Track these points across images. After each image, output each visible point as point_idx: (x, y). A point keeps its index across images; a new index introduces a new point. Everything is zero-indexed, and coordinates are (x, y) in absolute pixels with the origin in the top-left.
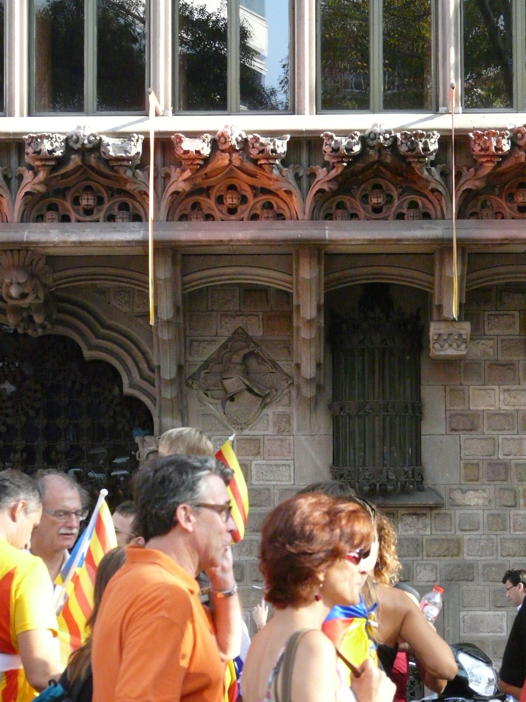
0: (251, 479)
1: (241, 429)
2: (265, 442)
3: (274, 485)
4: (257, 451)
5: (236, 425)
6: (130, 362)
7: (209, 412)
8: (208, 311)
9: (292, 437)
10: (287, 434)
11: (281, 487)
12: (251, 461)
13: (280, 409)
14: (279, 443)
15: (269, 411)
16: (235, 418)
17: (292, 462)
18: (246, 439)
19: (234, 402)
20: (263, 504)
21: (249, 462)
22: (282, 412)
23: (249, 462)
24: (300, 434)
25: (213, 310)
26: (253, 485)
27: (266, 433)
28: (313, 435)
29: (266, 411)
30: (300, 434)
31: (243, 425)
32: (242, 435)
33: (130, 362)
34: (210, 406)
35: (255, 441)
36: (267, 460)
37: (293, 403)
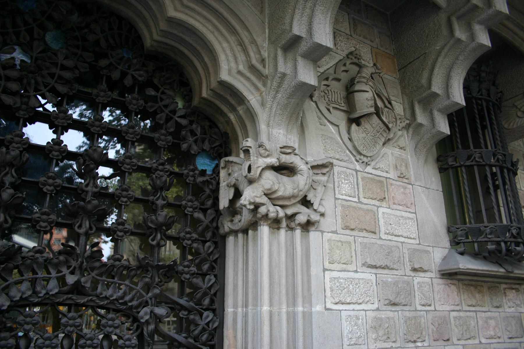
0: (380, 231)
2: (388, 186)
3: (402, 242)
5: (362, 157)
9: (410, 186)
10: (406, 181)
11: (409, 246)
12: (378, 207)
13: (397, 152)
14: (402, 190)
17: (415, 215)
19: (360, 127)
20: (395, 266)
26: (382, 239)
28: (428, 188)
31: (369, 158)
32: (365, 172)
34: (331, 126)
35: (381, 183)
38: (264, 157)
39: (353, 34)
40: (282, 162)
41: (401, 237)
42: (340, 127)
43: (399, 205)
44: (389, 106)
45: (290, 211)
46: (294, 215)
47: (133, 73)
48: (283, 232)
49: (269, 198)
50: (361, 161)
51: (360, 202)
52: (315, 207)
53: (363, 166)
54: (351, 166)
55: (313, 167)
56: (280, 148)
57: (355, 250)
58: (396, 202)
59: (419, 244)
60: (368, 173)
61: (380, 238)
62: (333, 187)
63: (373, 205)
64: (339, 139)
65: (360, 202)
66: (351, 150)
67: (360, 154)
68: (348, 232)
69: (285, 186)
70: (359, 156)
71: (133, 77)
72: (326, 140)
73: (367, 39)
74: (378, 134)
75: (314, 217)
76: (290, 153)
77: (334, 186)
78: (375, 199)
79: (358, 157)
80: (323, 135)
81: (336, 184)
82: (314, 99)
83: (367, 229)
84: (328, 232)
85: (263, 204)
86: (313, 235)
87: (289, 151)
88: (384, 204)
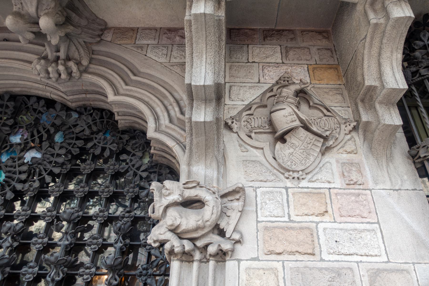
0: (321, 251)
1: (298, 178)
3: (357, 262)
4: (323, 209)
5: (291, 173)
6: (160, 110)
7: (254, 159)
8: (248, 62)
9: (368, 192)
11: (370, 266)
12: (317, 223)
15: (331, 158)
16: (289, 163)
18: (306, 193)
21: (314, 225)
22: (348, 160)
23: (314, 225)
24: (378, 187)
25: (254, 62)
26: (324, 260)
27: (332, 186)
28: (397, 190)
29: (328, 158)
30: (378, 187)
31: (300, 172)
32: (299, 187)
33: (160, 110)
34: (254, 150)
36: (340, 223)
37: (360, 151)
38: (167, 196)
39: (285, 61)
40: (186, 197)
41: (355, 256)
42: (264, 149)
43: (350, 216)
44: (328, 114)
45: (200, 244)
46: (206, 246)
47: (110, 146)
48: (195, 265)
49: (175, 233)
50: (291, 178)
51: (291, 221)
52: (228, 235)
53: (296, 182)
54: (282, 185)
55: (223, 196)
56: (184, 184)
57: (284, 278)
58: (344, 213)
59: (389, 262)
60: (302, 188)
61: (322, 260)
62: (255, 210)
63: (310, 222)
64: (264, 160)
65: (291, 221)
66: (277, 168)
67: (289, 171)
68: (273, 257)
69: (189, 220)
70: (287, 173)
71: (110, 149)
72: (248, 165)
73: (301, 60)
74: (310, 146)
75: (226, 246)
76: (194, 187)
77: (257, 208)
78: (312, 215)
79: (287, 174)
80: (243, 161)
81: (259, 207)
82: (234, 130)
83: (300, 251)
84: (247, 260)
85: (168, 241)
86: (230, 265)
87: (194, 185)
88: (326, 218)
